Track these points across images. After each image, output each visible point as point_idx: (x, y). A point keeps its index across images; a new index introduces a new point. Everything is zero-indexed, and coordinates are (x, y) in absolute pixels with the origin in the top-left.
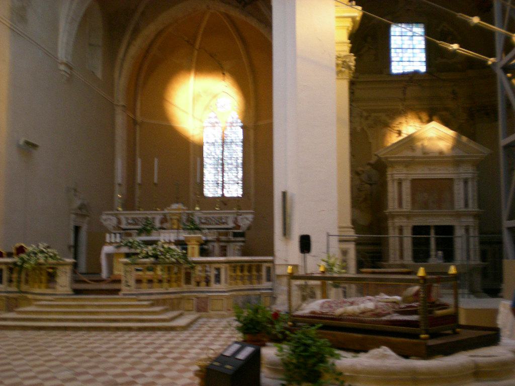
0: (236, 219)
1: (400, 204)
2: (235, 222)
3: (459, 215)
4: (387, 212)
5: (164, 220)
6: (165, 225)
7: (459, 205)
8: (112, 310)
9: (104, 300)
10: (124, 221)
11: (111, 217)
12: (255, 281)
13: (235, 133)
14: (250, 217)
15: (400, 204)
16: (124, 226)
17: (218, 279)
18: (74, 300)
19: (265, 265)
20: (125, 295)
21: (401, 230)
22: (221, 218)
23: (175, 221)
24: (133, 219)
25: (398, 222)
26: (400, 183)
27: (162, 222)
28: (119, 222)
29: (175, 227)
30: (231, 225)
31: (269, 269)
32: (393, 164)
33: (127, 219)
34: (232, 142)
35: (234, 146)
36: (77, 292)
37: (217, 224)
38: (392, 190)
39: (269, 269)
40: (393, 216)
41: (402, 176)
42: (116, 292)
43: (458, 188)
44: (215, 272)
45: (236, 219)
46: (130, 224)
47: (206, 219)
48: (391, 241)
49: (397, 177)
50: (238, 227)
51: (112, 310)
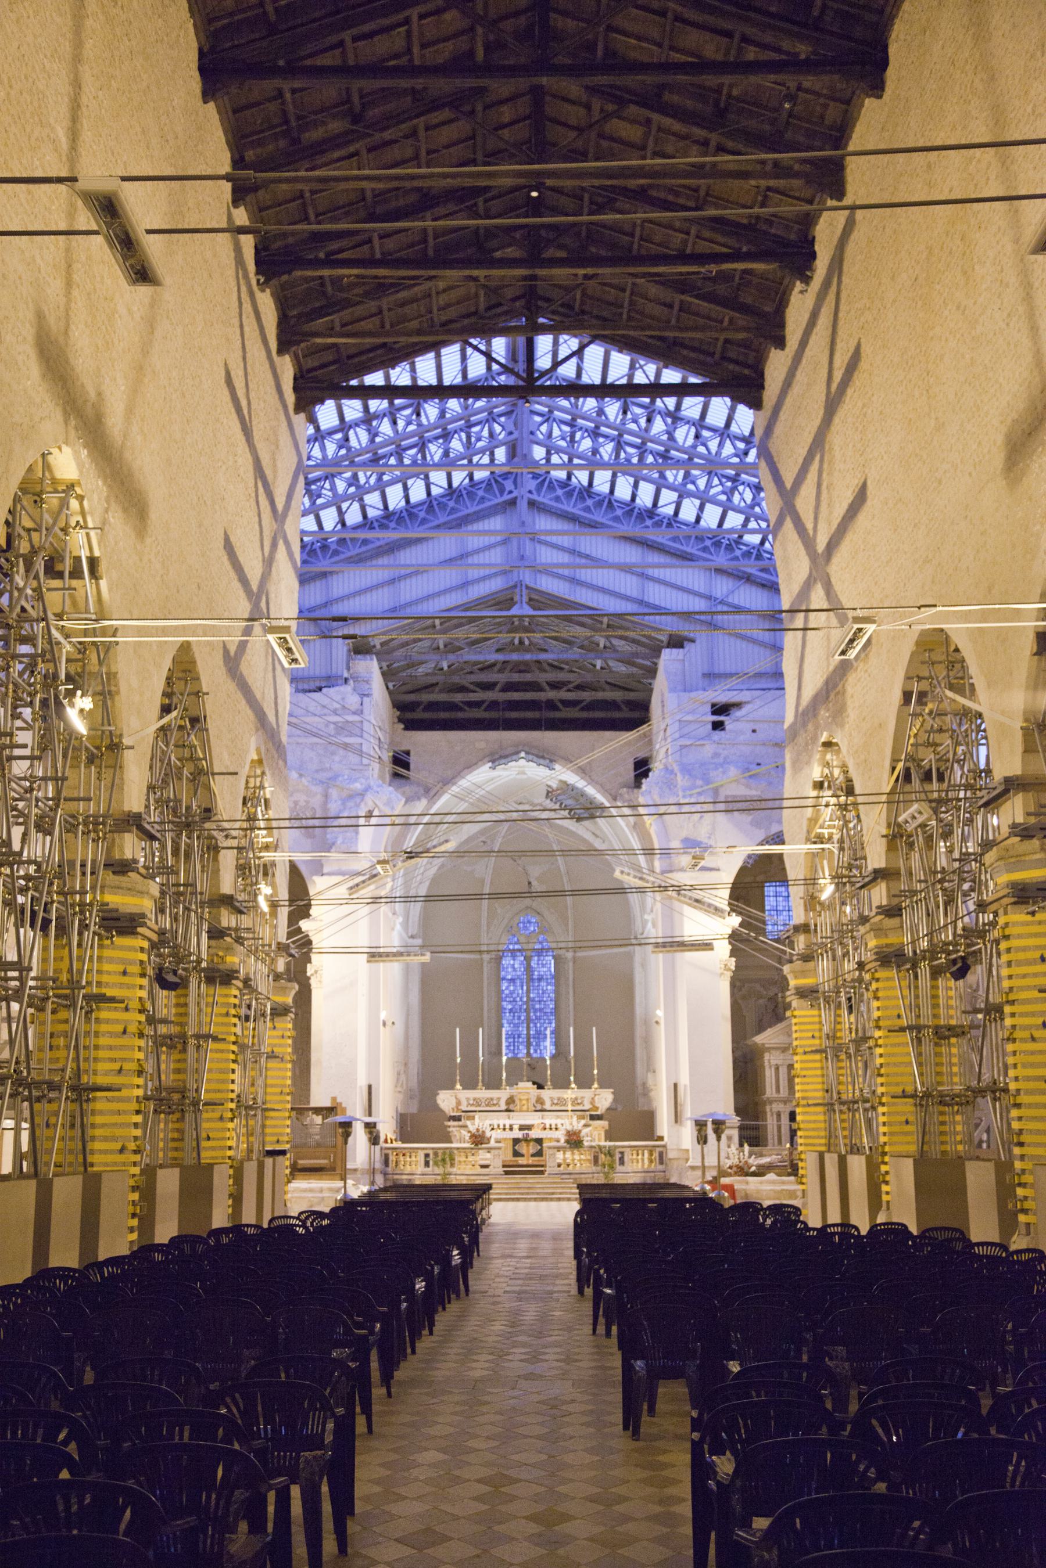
1: (778, 1090)
2: (592, 1102)
4: (765, 1097)
5: (511, 1100)
9: (531, 1179)
10: (464, 1103)
15: (778, 1090)
21: (779, 1115)
25: (776, 1107)
26: (777, 1069)
28: (459, 1103)
30: (587, 1106)
31: (661, 1154)
32: (769, 1049)
34: (540, 979)
35: (543, 984)
36: (507, 1173)
38: (769, 1074)
40: (771, 1103)
41: (779, 1062)
42: (542, 1172)
48: (769, 1128)
49: (773, 1062)
50: (597, 1108)
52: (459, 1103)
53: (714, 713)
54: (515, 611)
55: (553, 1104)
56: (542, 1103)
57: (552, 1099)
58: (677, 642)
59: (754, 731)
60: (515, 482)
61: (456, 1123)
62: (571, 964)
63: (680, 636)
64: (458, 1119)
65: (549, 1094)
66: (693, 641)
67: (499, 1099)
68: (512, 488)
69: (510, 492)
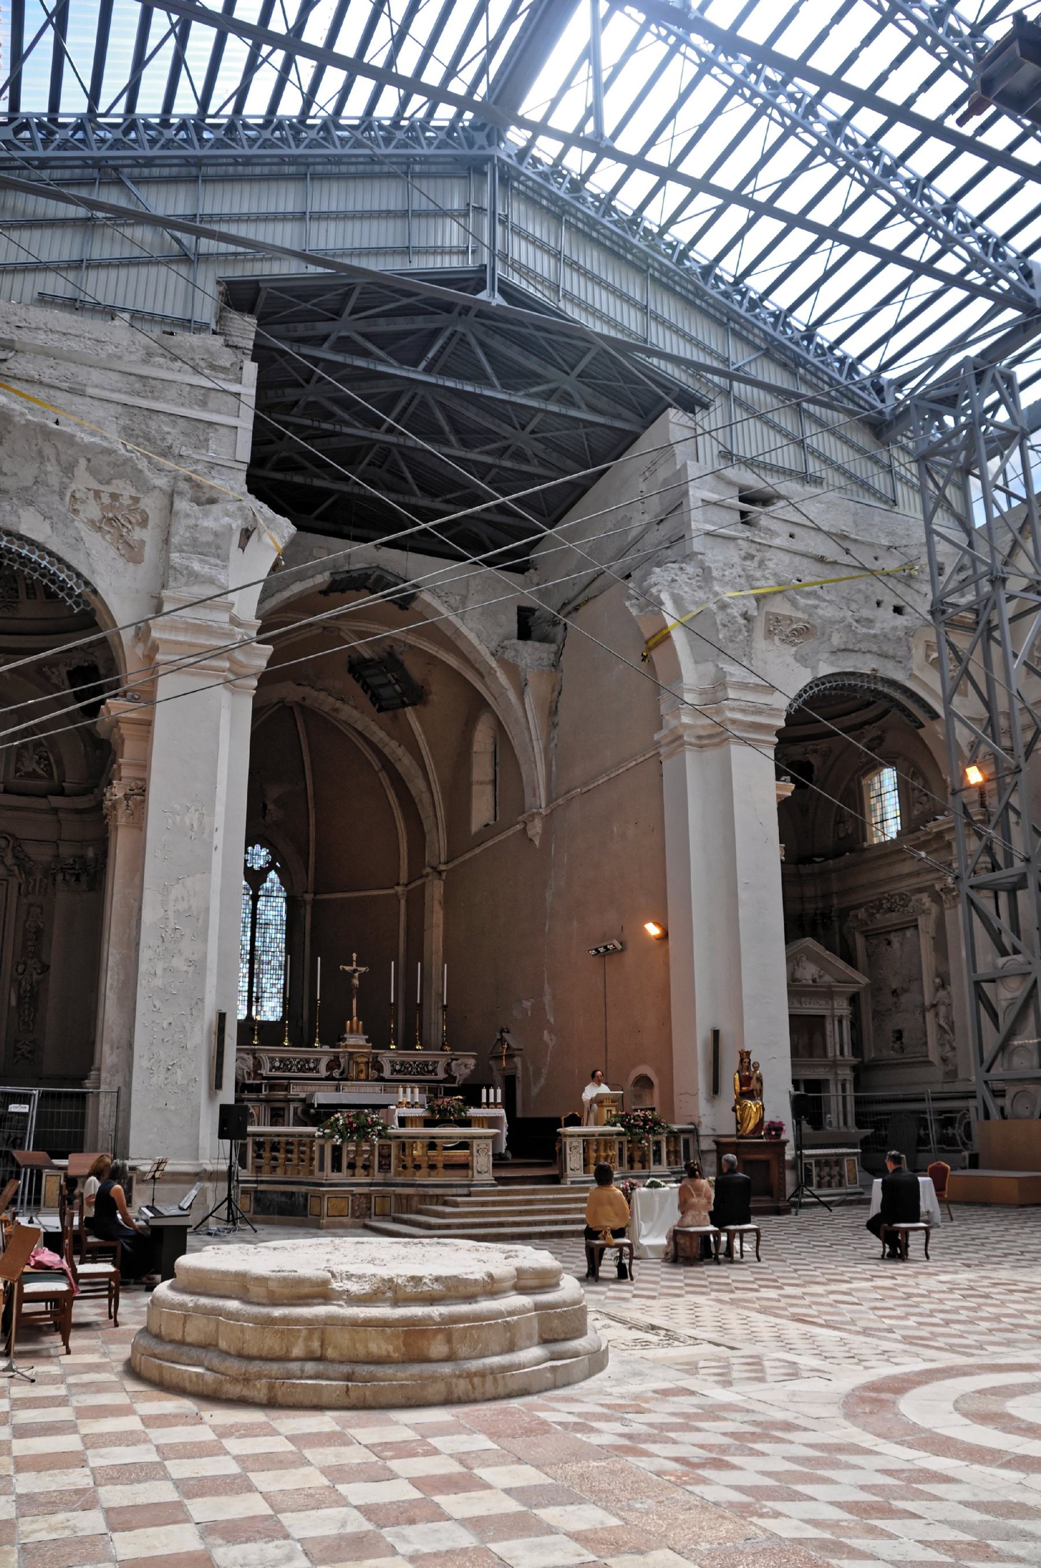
0: (449, 1065)
2: (448, 1068)
3: (834, 1065)
6: (336, 1073)
7: (833, 1050)
8: (573, 1206)
11: (246, 1056)
12: (638, 1165)
13: (273, 908)
14: (472, 1062)
16: (265, 1072)
17: (658, 1160)
18: (501, 1193)
19: (682, 1137)
20: (573, 1182)
22: (426, 1064)
23: (363, 1067)
24: (281, 1060)
27: (330, 1067)
28: (258, 1065)
29: (363, 1076)
31: (686, 1143)
33: (272, 1059)
35: (271, 931)
36: (500, 1181)
37: (419, 1073)
39: (686, 1143)
43: (831, 1028)
44: (653, 1148)
45: (449, 1065)
46: (278, 1069)
47: (402, 1064)
50: (451, 1079)
51: (573, 1206)
52: (258, 1065)
53: (742, 499)
54: (483, 296)
55: (394, 1071)
56: (380, 1068)
57: (393, 1063)
58: (690, 403)
59: (791, 536)
60: (489, 137)
61: (253, 1096)
62: (309, 908)
63: (693, 396)
64: (257, 1089)
65: (388, 1057)
66: (705, 406)
67: (317, 1061)
68: (485, 143)
69: (482, 147)
